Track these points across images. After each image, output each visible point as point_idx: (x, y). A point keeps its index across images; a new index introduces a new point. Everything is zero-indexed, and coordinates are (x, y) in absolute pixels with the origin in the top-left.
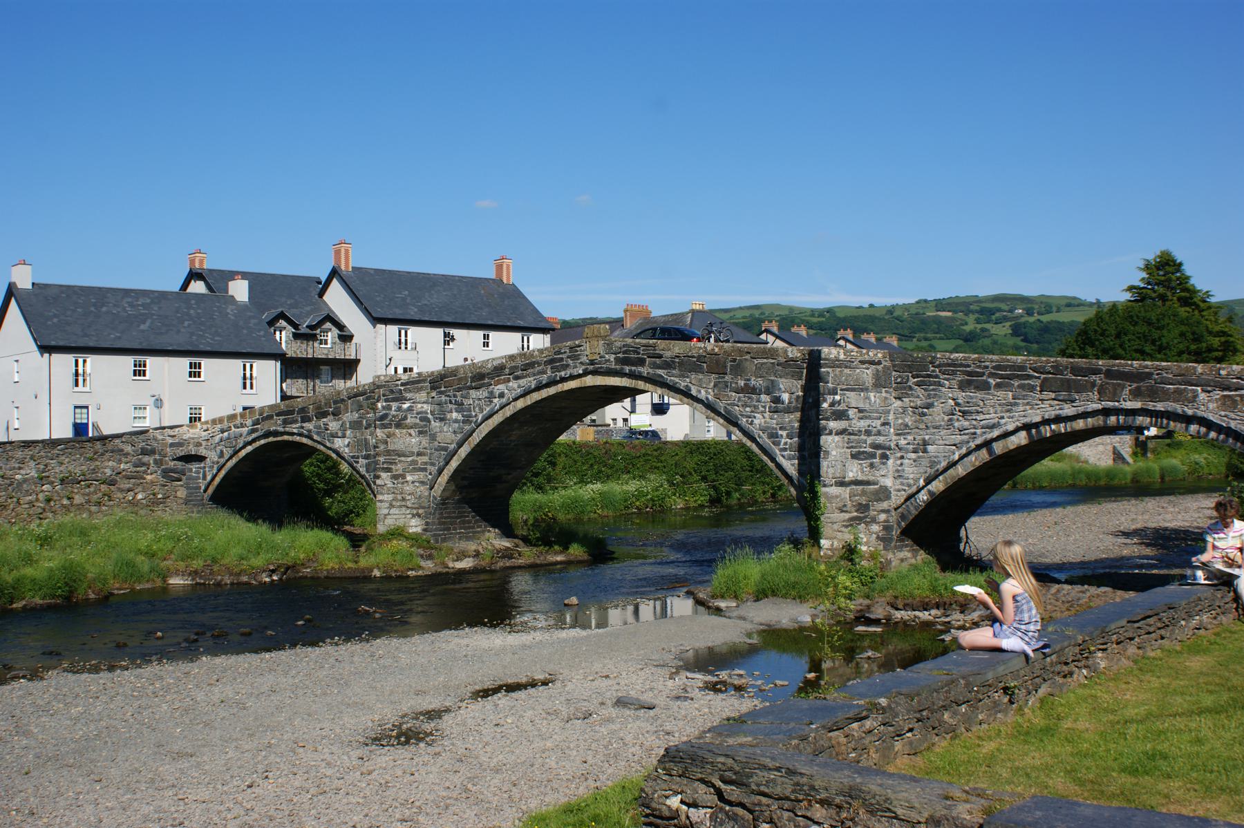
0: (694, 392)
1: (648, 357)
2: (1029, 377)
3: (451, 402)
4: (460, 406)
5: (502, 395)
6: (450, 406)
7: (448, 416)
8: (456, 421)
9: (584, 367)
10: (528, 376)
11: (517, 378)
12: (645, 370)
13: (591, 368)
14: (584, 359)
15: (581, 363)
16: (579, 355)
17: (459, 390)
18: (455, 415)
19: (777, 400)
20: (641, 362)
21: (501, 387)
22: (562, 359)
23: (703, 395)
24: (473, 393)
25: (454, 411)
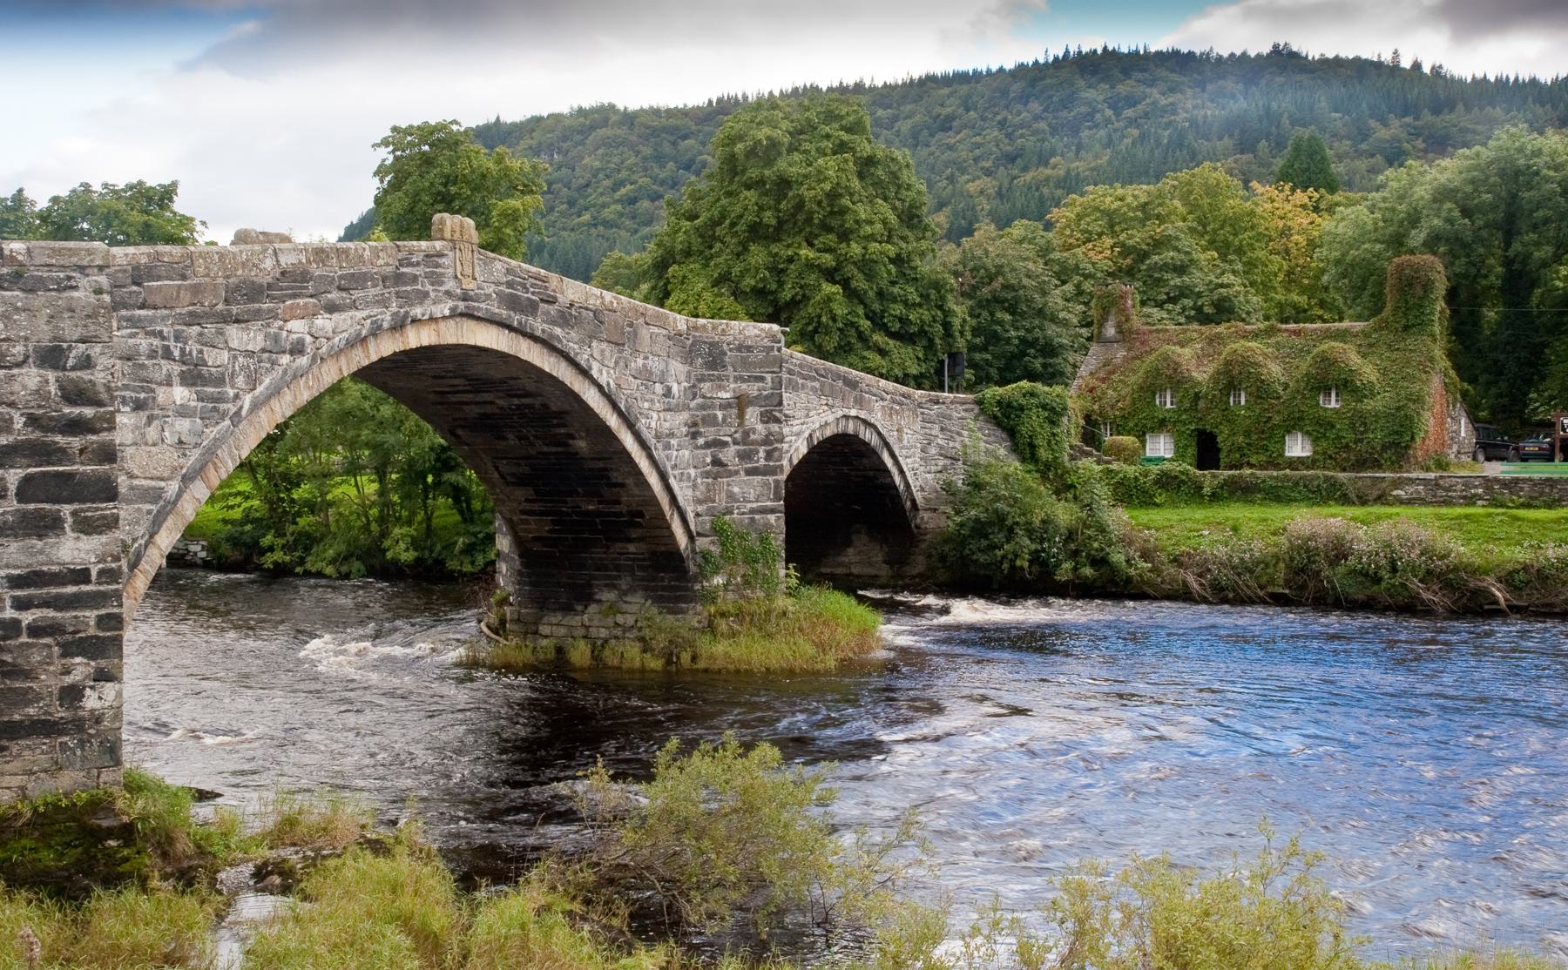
0: (595, 373)
1: (542, 300)
2: (814, 379)
3: (168, 355)
4: (194, 376)
5: (297, 349)
6: (166, 365)
7: (162, 394)
8: (183, 412)
9: (450, 304)
10: (354, 306)
11: (332, 308)
12: (539, 326)
13: (462, 305)
14: (450, 285)
15: (448, 293)
16: (442, 275)
17: (193, 319)
18: (180, 394)
19: (668, 393)
20: (531, 308)
21: (298, 327)
22: (415, 278)
23: (603, 380)
24: (234, 334)
25: (176, 380)
